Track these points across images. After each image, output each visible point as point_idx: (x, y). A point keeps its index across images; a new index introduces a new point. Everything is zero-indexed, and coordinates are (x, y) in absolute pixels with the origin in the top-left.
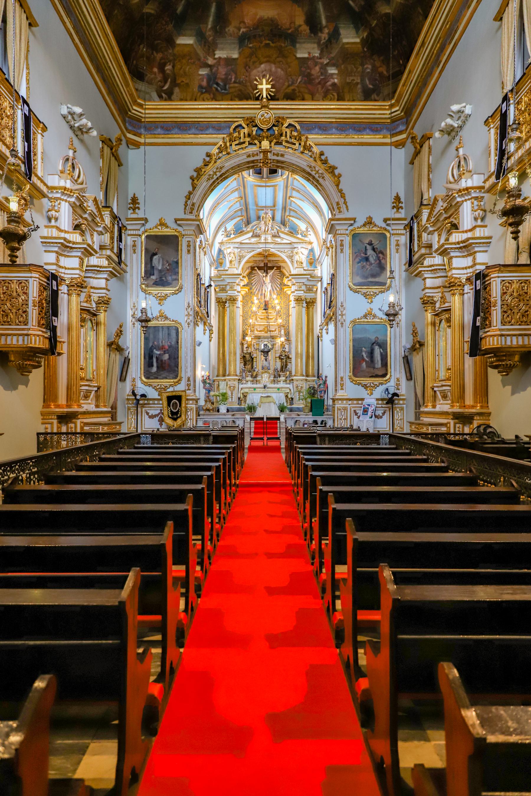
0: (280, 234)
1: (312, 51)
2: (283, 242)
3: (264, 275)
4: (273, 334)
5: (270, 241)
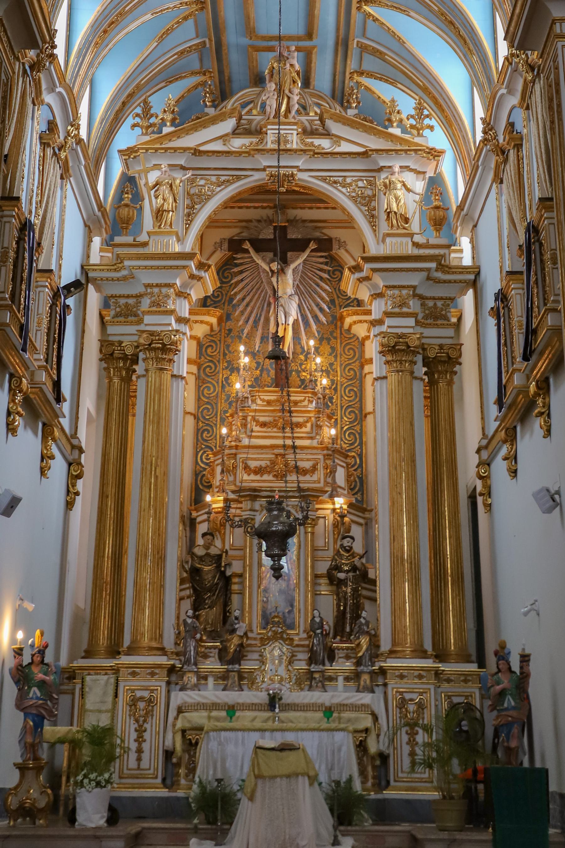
0: (330, 123)
2: (338, 150)
3: (275, 266)
4: (308, 482)
5: (295, 146)
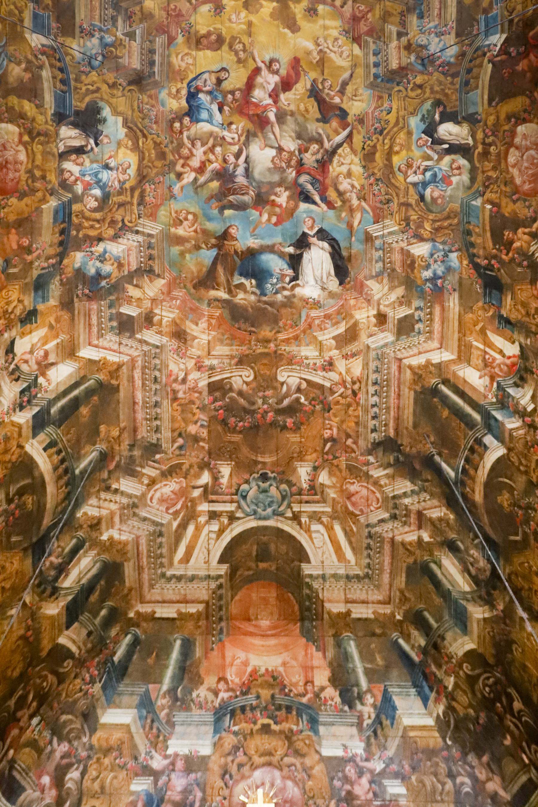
1: (349, 743)
